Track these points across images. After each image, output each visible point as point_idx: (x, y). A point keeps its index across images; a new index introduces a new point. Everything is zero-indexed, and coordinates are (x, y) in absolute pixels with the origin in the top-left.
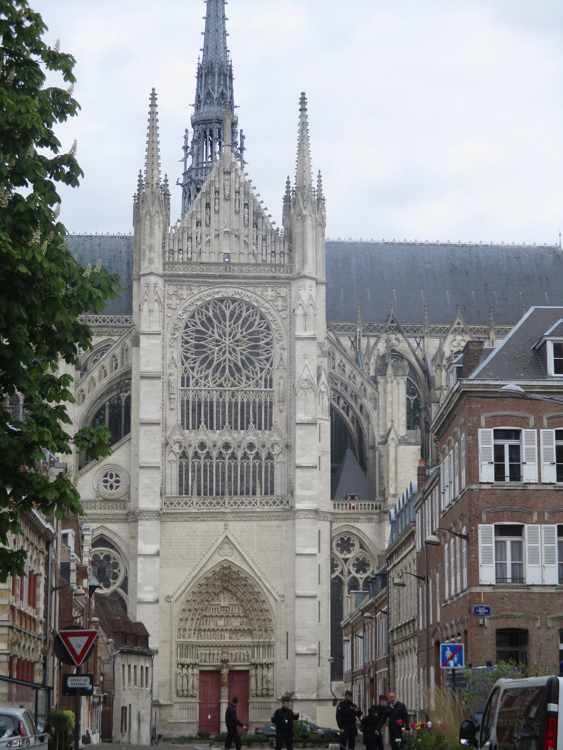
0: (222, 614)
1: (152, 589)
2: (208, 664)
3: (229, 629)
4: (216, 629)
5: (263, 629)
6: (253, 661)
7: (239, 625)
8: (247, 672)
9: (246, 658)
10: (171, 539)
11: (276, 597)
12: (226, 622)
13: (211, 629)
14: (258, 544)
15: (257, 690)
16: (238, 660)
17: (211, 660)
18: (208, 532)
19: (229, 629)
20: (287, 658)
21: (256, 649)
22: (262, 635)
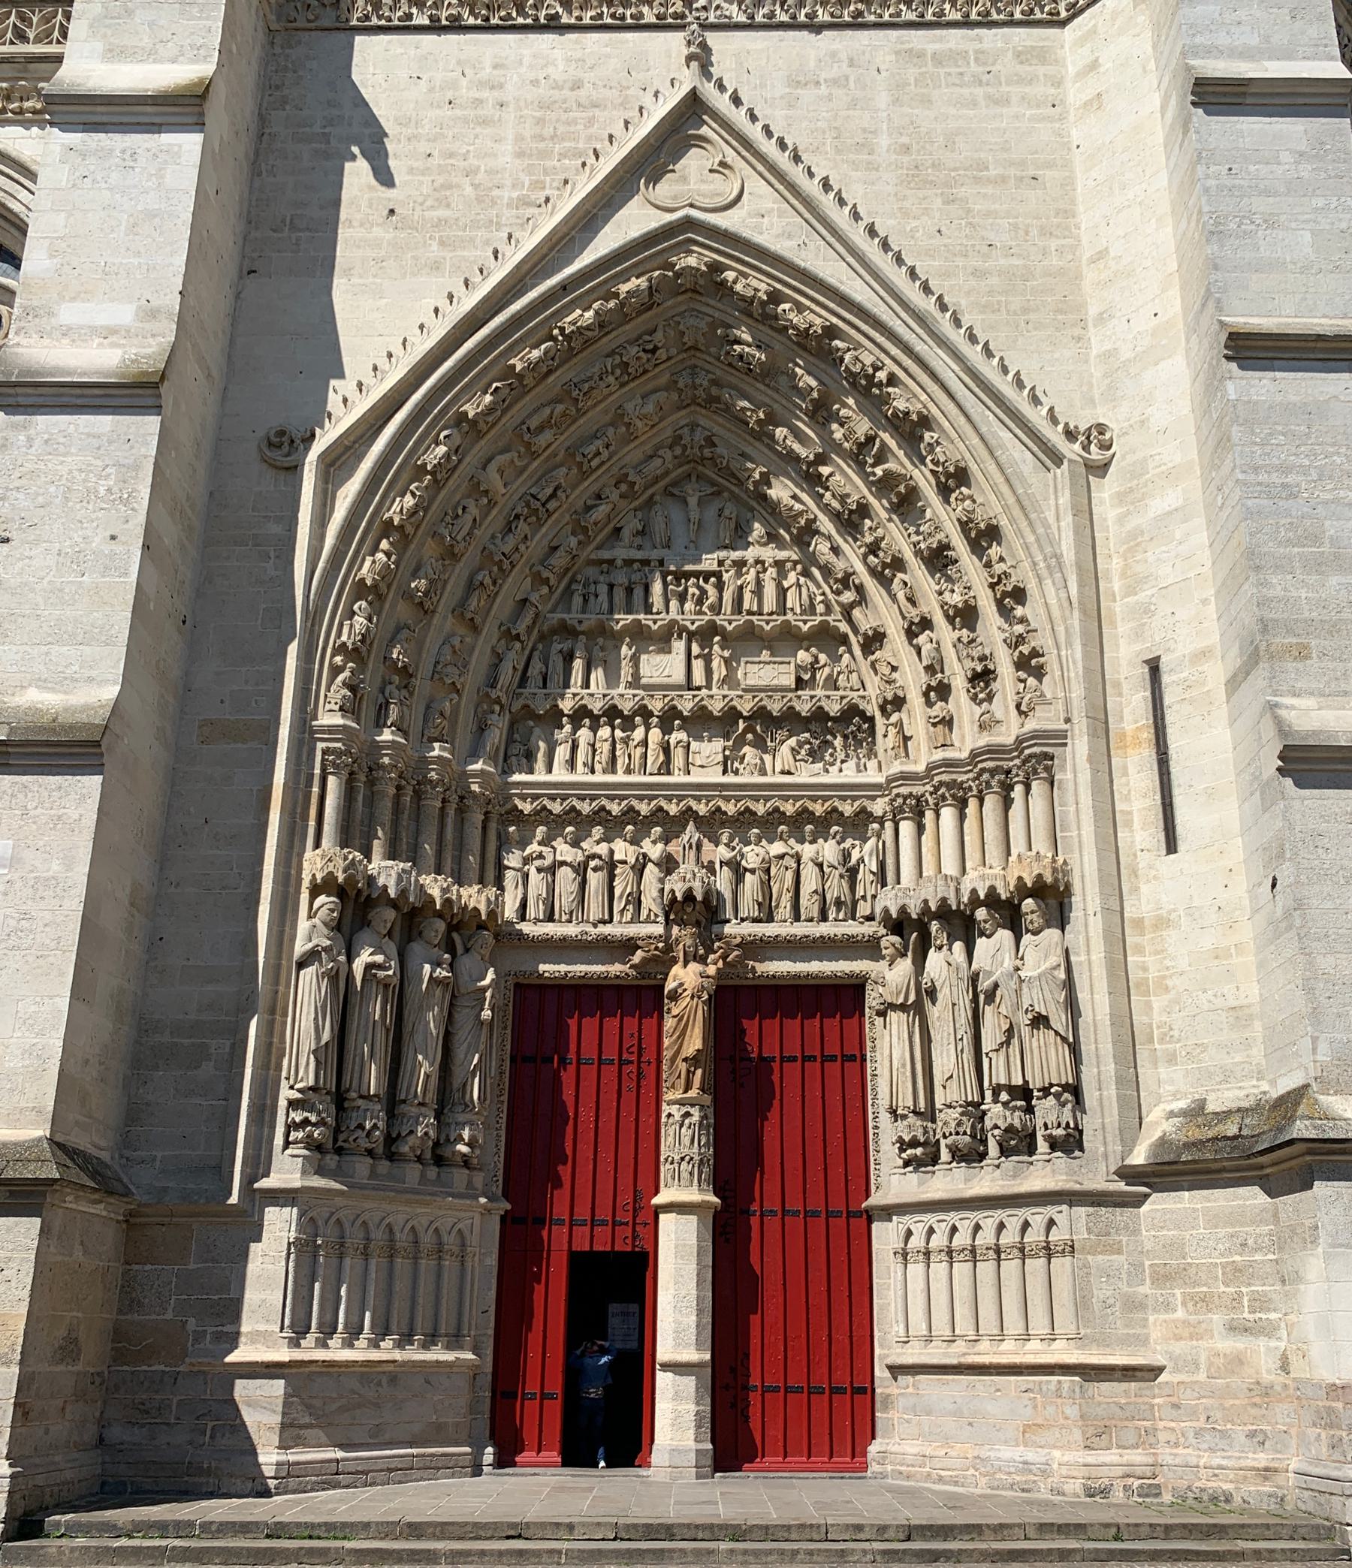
0: (674, 614)
1: (124, 314)
2: (571, 930)
3: (716, 707)
4: (626, 707)
5: (959, 683)
6: (889, 900)
7: (789, 681)
8: (852, 992)
9: (836, 888)
10: (330, 122)
11: (1055, 436)
12: (698, 666)
13: (596, 707)
14: (906, 149)
15: (929, 1114)
16: (784, 910)
17: (595, 908)
18: (577, 86)
19: (716, 707)
20: (1171, 847)
21: (906, 828)
22: (948, 722)
